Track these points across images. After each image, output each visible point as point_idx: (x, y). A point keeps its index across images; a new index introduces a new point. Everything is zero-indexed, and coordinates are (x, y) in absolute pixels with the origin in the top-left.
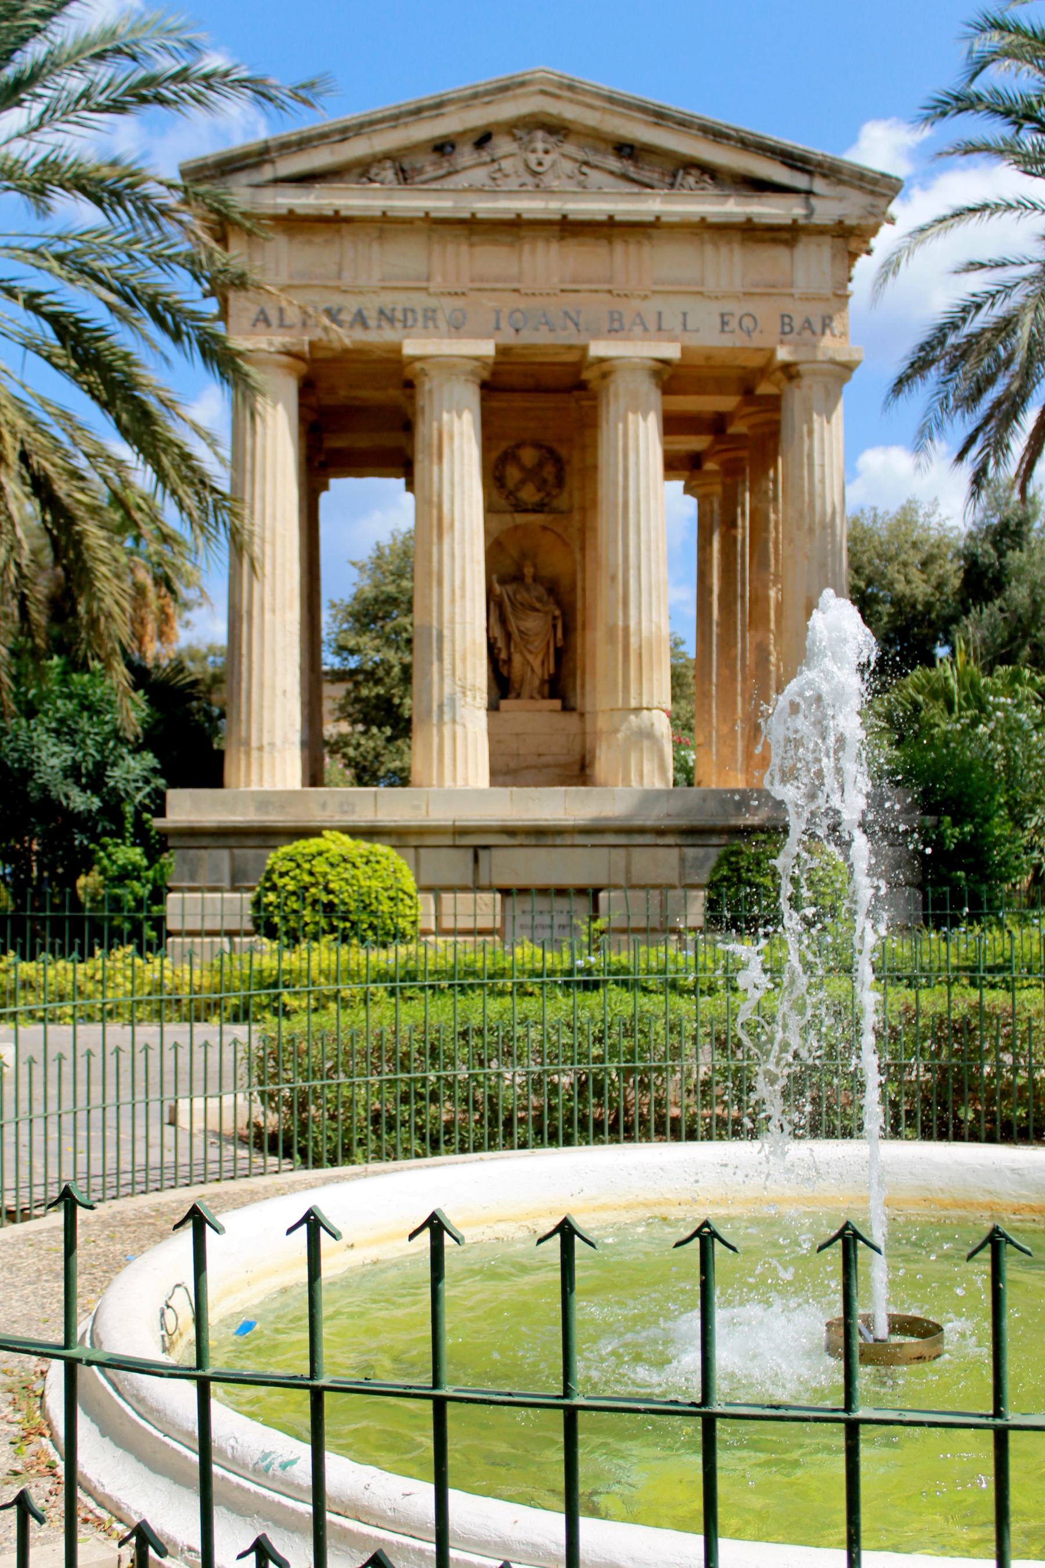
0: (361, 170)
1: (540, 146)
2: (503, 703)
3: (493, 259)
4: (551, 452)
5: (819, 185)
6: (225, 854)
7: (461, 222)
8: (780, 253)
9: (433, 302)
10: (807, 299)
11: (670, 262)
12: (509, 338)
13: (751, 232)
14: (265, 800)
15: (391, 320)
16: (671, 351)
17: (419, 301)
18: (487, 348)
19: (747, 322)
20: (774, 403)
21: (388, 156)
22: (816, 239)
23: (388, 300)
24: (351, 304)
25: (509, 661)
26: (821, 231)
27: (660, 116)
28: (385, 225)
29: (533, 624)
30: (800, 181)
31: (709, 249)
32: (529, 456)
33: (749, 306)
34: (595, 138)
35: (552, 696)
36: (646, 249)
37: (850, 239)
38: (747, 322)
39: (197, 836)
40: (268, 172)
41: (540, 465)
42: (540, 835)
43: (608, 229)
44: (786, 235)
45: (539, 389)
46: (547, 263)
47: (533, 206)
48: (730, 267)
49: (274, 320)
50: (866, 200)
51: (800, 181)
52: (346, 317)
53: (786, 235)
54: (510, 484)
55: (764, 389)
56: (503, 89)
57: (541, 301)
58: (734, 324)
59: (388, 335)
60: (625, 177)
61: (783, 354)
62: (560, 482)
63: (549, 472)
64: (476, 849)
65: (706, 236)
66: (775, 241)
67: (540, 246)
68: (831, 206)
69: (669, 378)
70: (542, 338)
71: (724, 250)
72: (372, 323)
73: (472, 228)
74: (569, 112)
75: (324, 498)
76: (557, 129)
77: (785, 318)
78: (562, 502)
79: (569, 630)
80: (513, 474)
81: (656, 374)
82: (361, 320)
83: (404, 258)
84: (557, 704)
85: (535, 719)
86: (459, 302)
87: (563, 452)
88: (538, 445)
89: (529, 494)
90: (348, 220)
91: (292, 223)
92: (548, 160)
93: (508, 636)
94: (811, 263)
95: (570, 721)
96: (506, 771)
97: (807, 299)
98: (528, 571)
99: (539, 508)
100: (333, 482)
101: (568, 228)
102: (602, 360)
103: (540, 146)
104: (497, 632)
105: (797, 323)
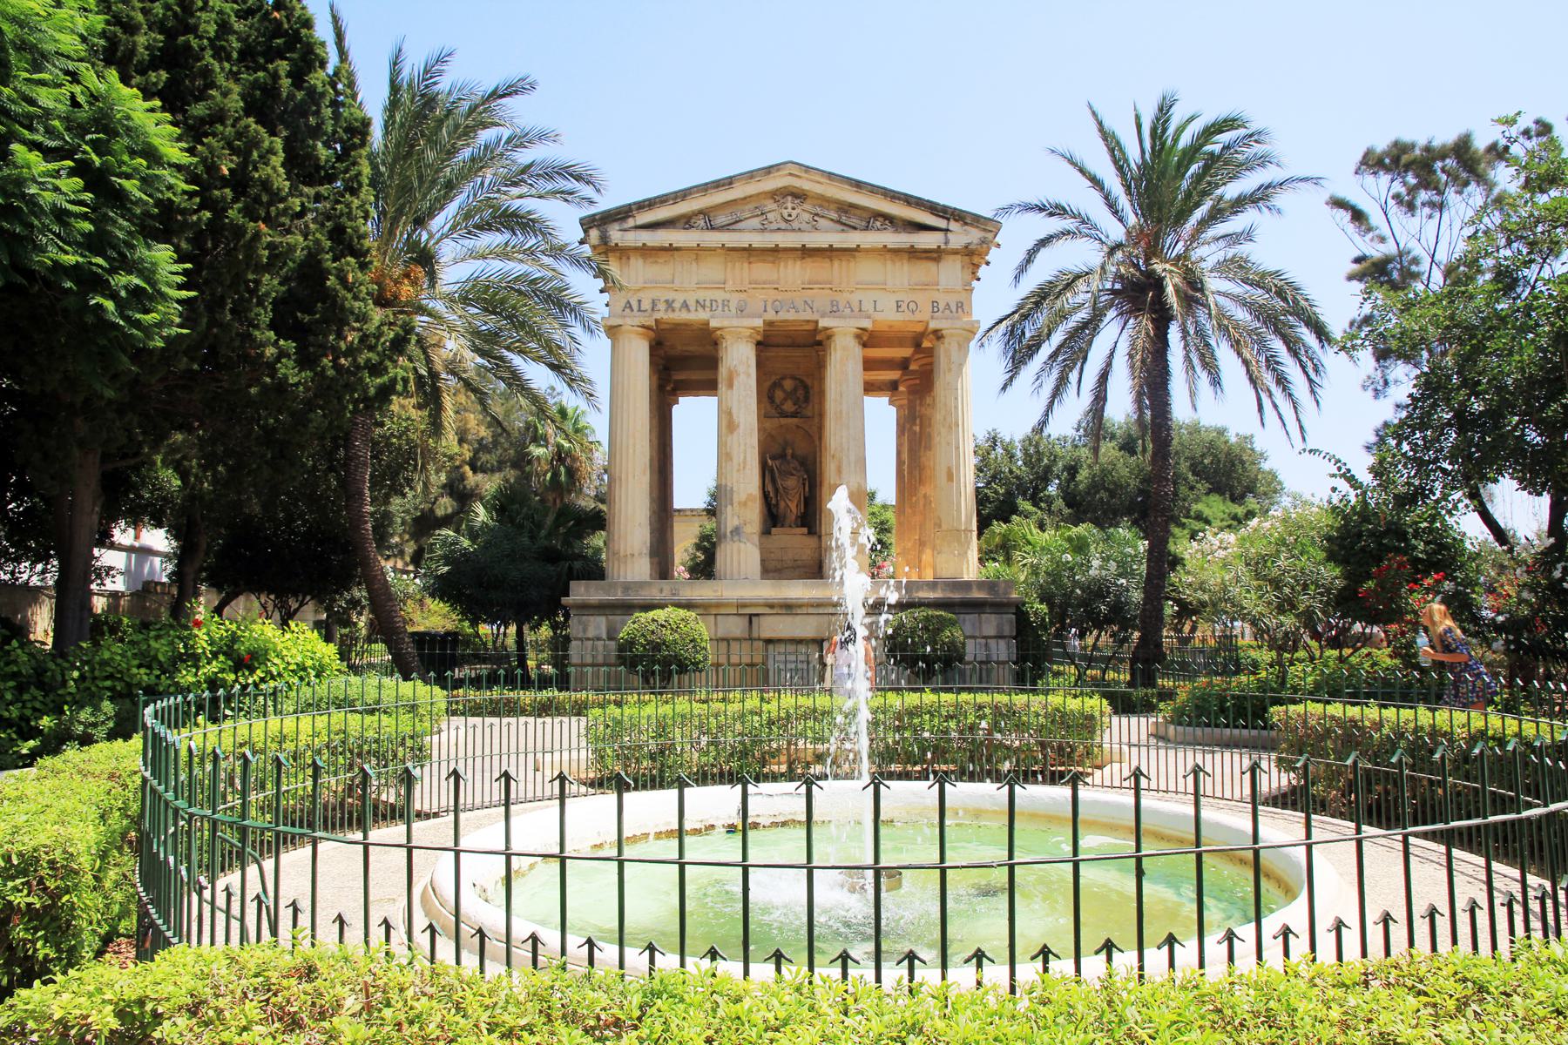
0: (685, 222)
1: (790, 205)
2: (774, 530)
3: (762, 270)
4: (802, 381)
5: (953, 226)
6: (603, 619)
7: (744, 249)
8: (931, 266)
9: (727, 296)
10: (947, 291)
11: (866, 270)
12: (771, 316)
13: (913, 253)
14: (627, 587)
15: (703, 307)
16: (867, 324)
17: (719, 295)
18: (758, 323)
19: (912, 306)
20: (930, 352)
21: (701, 212)
22: (952, 257)
23: (701, 295)
25: (777, 505)
26: (955, 252)
27: (858, 185)
28: (699, 251)
30: (942, 223)
31: (889, 263)
33: (913, 297)
34: (825, 201)
35: (803, 526)
36: (852, 264)
38: (912, 306)
40: (631, 222)
41: (795, 390)
42: (788, 608)
43: (830, 252)
44: (935, 255)
45: (794, 345)
46: (794, 273)
48: (902, 274)
49: (635, 307)
50: (982, 234)
51: (942, 223)
52: (677, 305)
53: (935, 255)
54: (777, 401)
55: (926, 344)
56: (768, 170)
57: (793, 295)
58: (904, 307)
60: (839, 222)
61: (933, 325)
62: (807, 399)
63: (800, 393)
64: (751, 616)
65: (888, 256)
66: (927, 258)
67: (790, 263)
68: (960, 237)
70: (793, 315)
71: (898, 264)
72: (692, 308)
73: (749, 252)
74: (805, 185)
75: (676, 411)
76: (799, 196)
80: (779, 395)
81: (858, 337)
82: (685, 305)
83: (712, 270)
84: (805, 530)
85: (792, 541)
86: (743, 296)
87: (809, 382)
88: (793, 378)
89: (789, 407)
90: (678, 249)
91: (646, 251)
92: (794, 213)
93: (776, 491)
94: (950, 271)
95: (811, 542)
96: (772, 569)
97: (947, 291)
98: (789, 451)
99: (794, 415)
100: (681, 399)
101: (806, 252)
102: (826, 329)
103: (790, 205)
104: (770, 488)
105: (941, 307)
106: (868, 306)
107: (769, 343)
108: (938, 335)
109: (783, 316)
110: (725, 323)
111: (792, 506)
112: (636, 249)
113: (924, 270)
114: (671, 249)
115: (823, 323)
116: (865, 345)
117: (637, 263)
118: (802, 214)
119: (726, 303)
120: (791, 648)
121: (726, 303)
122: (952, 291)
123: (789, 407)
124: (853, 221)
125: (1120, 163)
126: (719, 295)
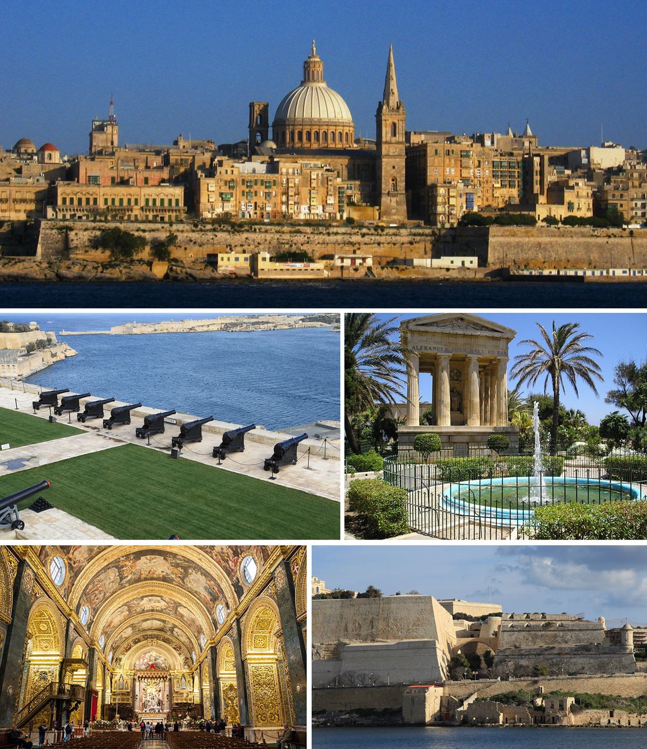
3: (452, 340)
8: (498, 342)
12: (454, 353)
13: (493, 338)
16: (480, 356)
17: (440, 346)
18: (451, 354)
23: (435, 346)
24: (429, 346)
28: (434, 334)
29: (455, 399)
32: (455, 371)
37: (509, 340)
39: (403, 433)
45: (457, 361)
46: (461, 341)
47: (460, 332)
52: (428, 348)
59: (435, 351)
61: (498, 358)
63: (459, 374)
69: (479, 360)
73: (449, 335)
77: (499, 352)
78: (460, 379)
79: (462, 400)
82: (430, 348)
87: (461, 371)
89: (455, 378)
94: (502, 343)
98: (455, 390)
101: (464, 335)
106: (481, 352)
107: (453, 360)
108: (499, 360)
109: (458, 353)
110: (442, 354)
111: (457, 407)
112: (416, 331)
113: (494, 343)
114: (427, 332)
115: (469, 355)
116: (479, 362)
117: (416, 335)
118: (463, 324)
119: (442, 348)
120: (461, 444)
121: (442, 348)
122: (503, 349)
123: (455, 378)
124: (477, 328)
125: (549, 342)
126: (440, 346)
